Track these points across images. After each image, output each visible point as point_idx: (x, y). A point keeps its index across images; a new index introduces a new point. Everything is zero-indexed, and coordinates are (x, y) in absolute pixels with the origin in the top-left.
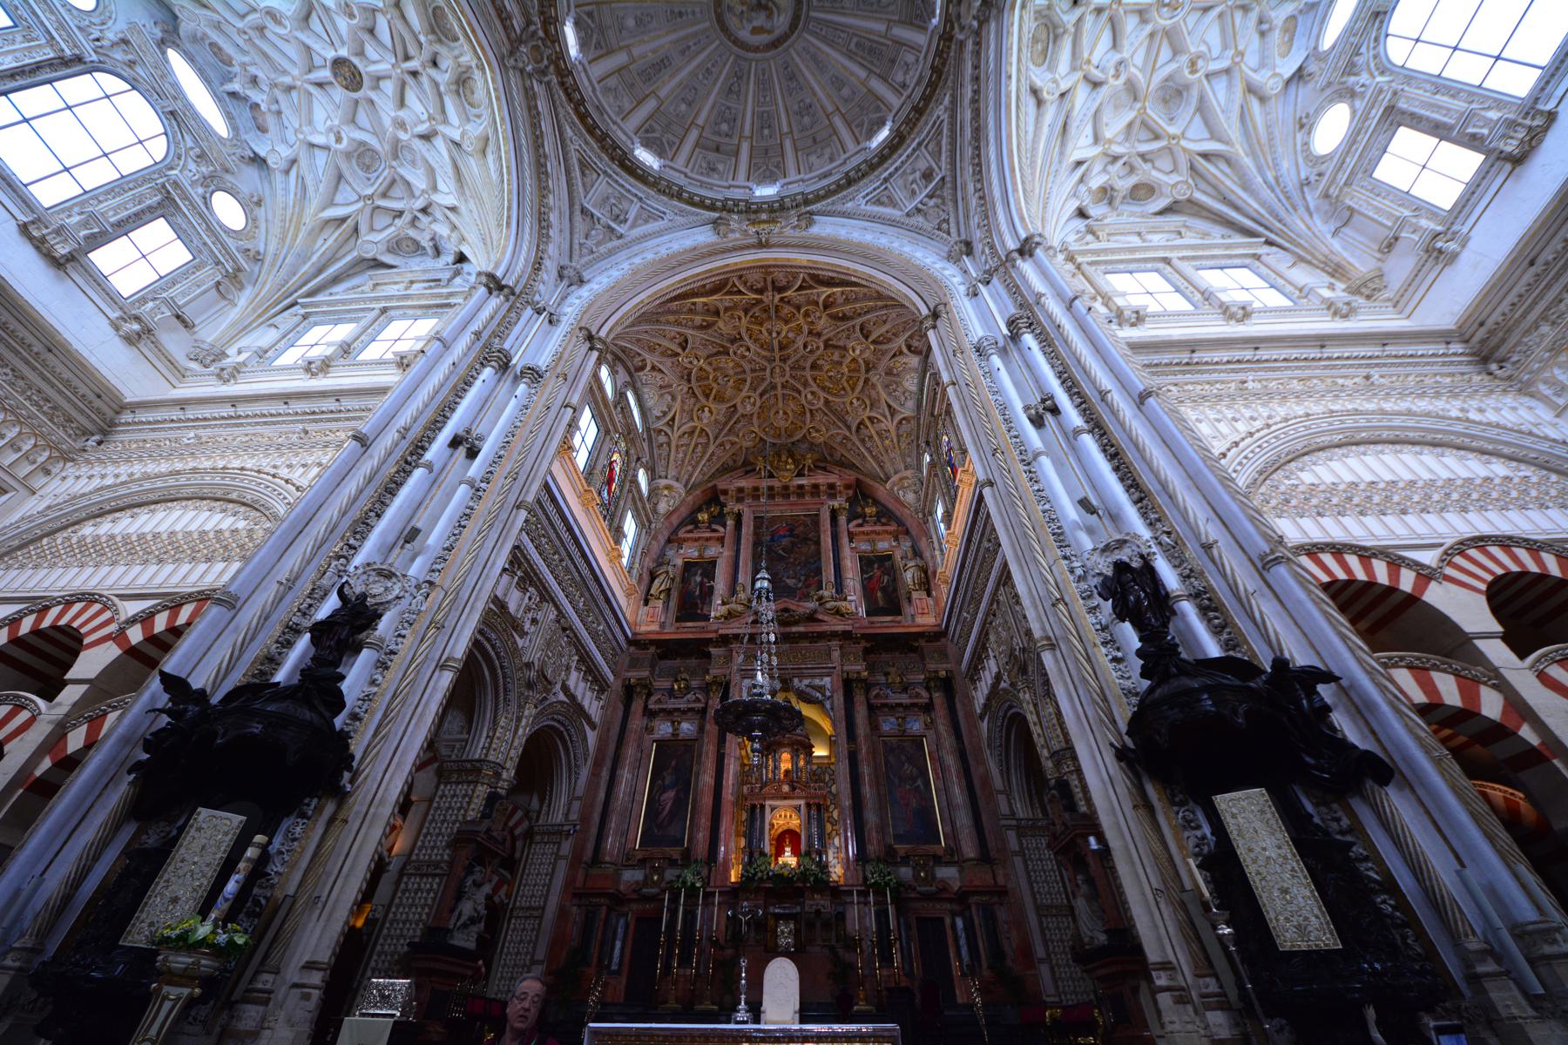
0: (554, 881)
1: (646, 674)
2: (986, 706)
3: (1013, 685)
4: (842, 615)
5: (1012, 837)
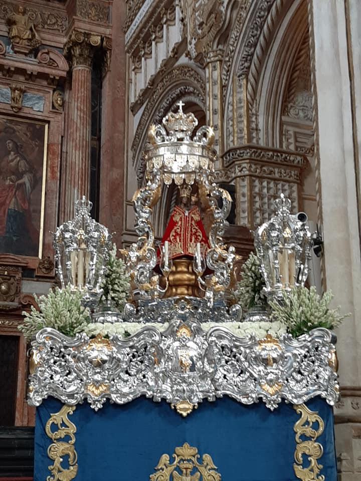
3: (200, 60)
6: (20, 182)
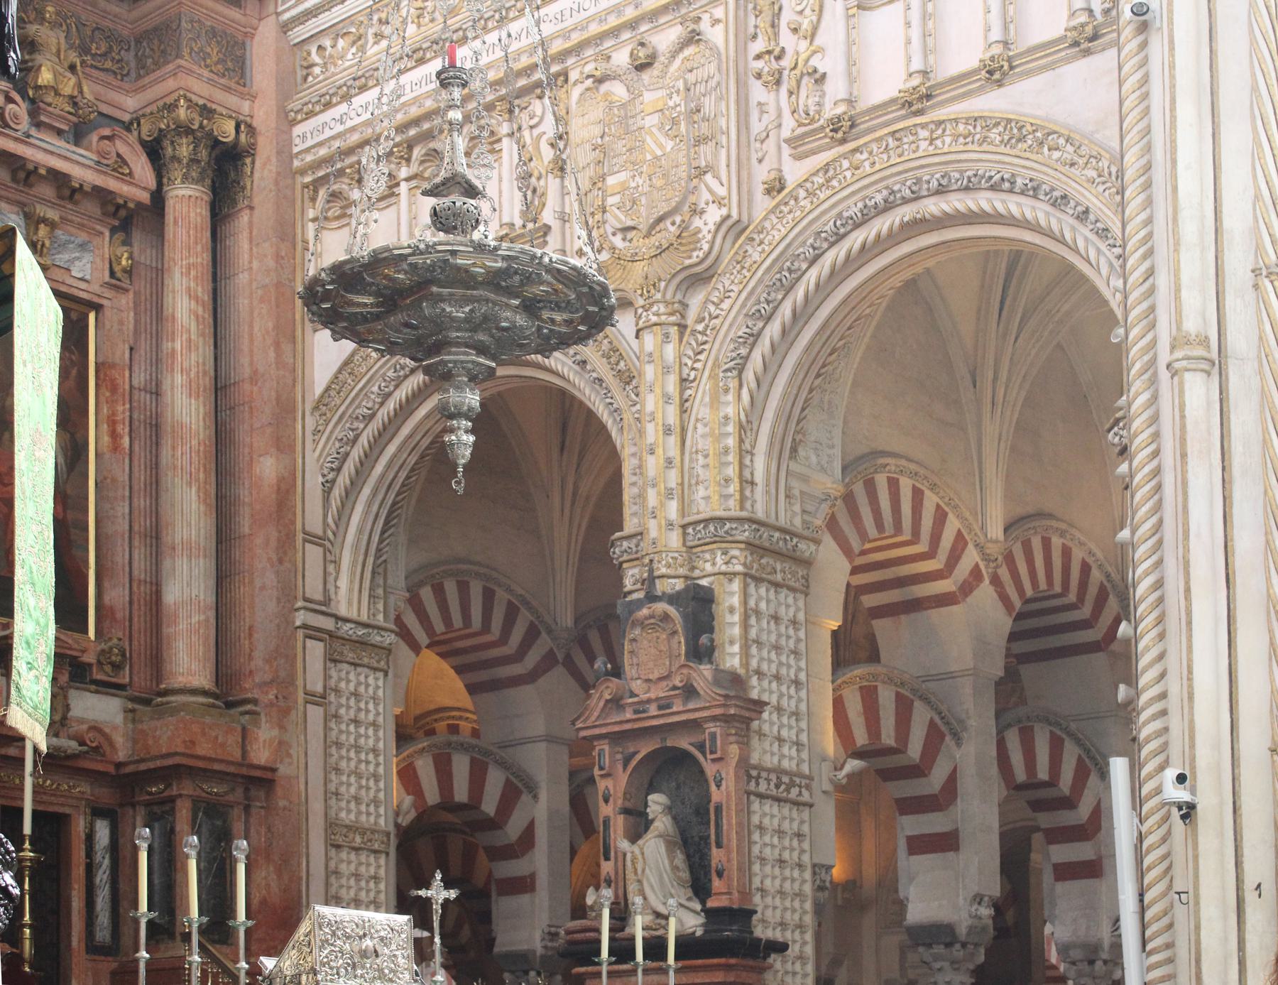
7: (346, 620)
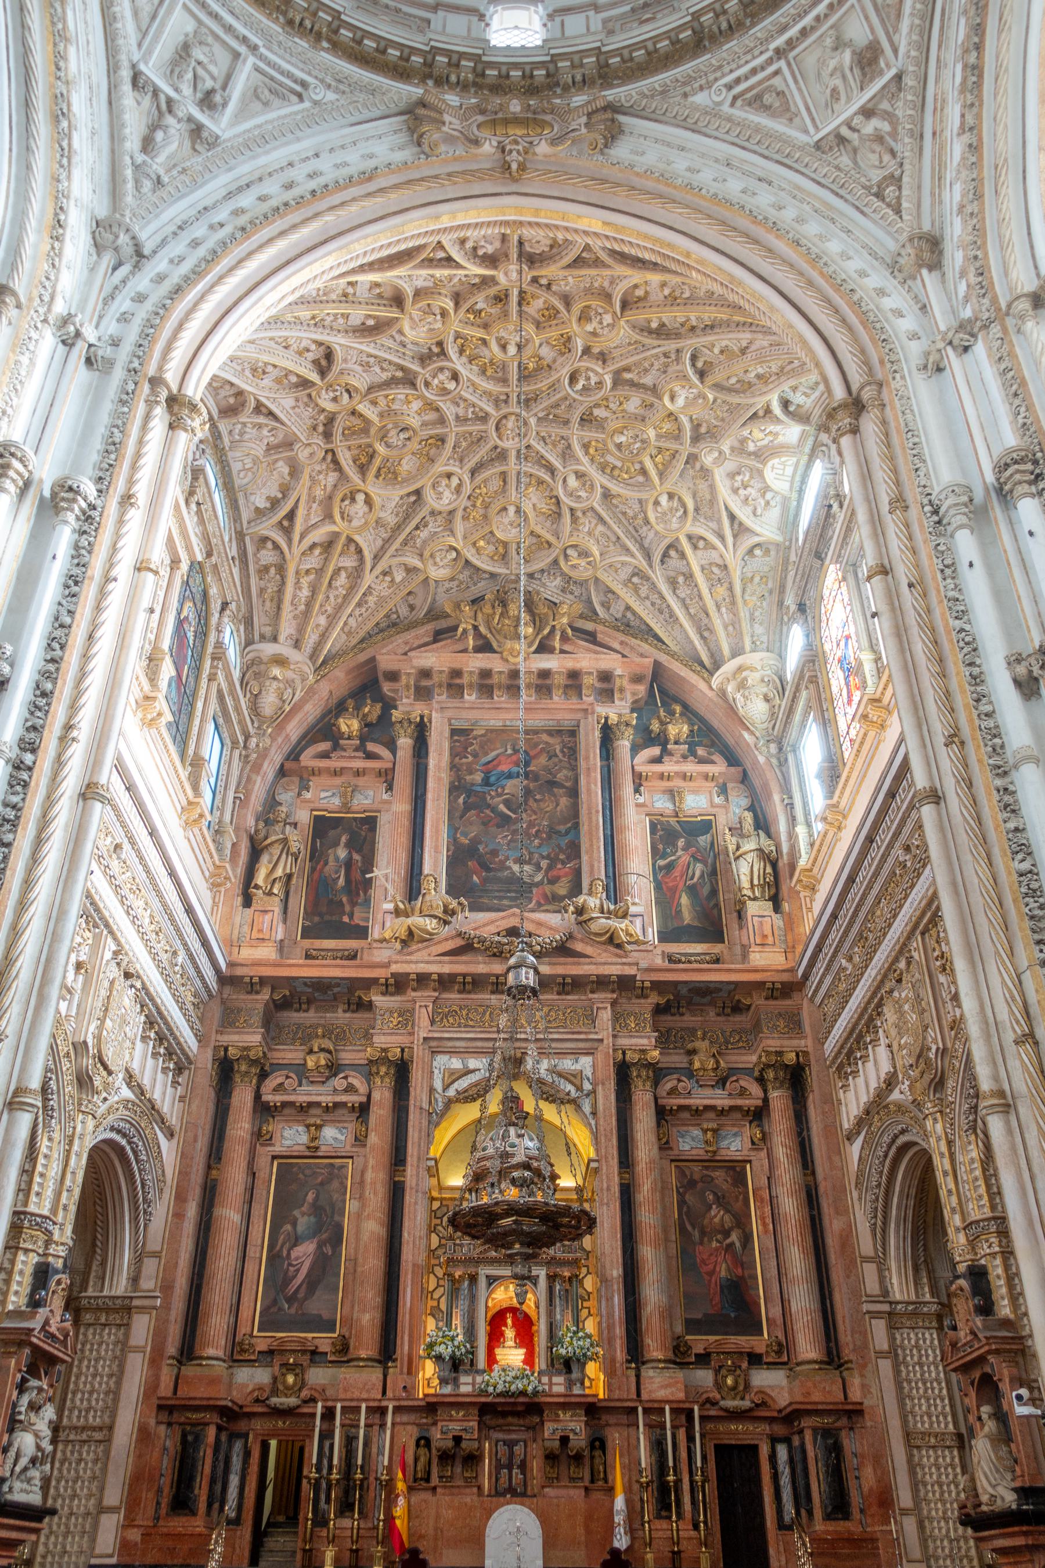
0: (125, 1386)
1: (253, 1038)
2: (860, 1123)
4: (619, 946)
5: (879, 1333)
6: (728, 1241)
7: (898, 1303)
